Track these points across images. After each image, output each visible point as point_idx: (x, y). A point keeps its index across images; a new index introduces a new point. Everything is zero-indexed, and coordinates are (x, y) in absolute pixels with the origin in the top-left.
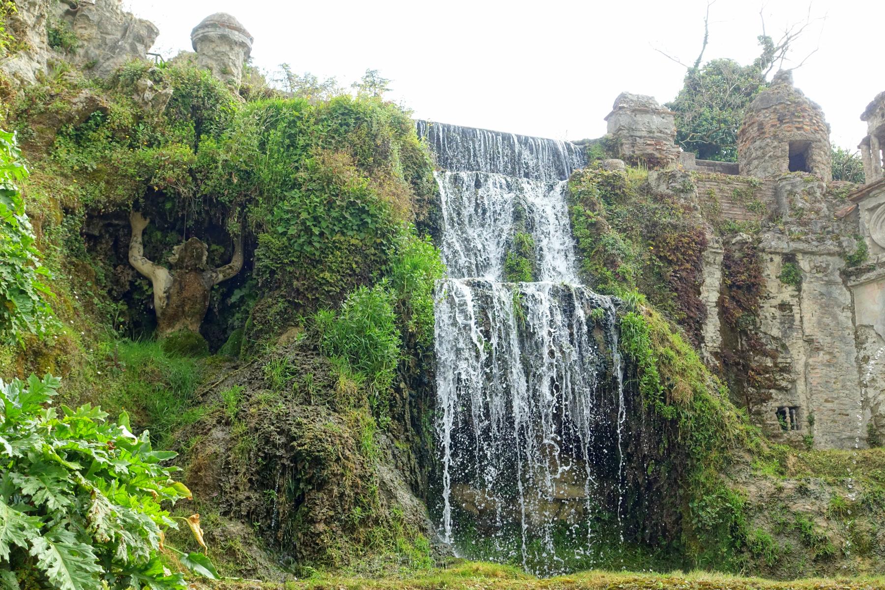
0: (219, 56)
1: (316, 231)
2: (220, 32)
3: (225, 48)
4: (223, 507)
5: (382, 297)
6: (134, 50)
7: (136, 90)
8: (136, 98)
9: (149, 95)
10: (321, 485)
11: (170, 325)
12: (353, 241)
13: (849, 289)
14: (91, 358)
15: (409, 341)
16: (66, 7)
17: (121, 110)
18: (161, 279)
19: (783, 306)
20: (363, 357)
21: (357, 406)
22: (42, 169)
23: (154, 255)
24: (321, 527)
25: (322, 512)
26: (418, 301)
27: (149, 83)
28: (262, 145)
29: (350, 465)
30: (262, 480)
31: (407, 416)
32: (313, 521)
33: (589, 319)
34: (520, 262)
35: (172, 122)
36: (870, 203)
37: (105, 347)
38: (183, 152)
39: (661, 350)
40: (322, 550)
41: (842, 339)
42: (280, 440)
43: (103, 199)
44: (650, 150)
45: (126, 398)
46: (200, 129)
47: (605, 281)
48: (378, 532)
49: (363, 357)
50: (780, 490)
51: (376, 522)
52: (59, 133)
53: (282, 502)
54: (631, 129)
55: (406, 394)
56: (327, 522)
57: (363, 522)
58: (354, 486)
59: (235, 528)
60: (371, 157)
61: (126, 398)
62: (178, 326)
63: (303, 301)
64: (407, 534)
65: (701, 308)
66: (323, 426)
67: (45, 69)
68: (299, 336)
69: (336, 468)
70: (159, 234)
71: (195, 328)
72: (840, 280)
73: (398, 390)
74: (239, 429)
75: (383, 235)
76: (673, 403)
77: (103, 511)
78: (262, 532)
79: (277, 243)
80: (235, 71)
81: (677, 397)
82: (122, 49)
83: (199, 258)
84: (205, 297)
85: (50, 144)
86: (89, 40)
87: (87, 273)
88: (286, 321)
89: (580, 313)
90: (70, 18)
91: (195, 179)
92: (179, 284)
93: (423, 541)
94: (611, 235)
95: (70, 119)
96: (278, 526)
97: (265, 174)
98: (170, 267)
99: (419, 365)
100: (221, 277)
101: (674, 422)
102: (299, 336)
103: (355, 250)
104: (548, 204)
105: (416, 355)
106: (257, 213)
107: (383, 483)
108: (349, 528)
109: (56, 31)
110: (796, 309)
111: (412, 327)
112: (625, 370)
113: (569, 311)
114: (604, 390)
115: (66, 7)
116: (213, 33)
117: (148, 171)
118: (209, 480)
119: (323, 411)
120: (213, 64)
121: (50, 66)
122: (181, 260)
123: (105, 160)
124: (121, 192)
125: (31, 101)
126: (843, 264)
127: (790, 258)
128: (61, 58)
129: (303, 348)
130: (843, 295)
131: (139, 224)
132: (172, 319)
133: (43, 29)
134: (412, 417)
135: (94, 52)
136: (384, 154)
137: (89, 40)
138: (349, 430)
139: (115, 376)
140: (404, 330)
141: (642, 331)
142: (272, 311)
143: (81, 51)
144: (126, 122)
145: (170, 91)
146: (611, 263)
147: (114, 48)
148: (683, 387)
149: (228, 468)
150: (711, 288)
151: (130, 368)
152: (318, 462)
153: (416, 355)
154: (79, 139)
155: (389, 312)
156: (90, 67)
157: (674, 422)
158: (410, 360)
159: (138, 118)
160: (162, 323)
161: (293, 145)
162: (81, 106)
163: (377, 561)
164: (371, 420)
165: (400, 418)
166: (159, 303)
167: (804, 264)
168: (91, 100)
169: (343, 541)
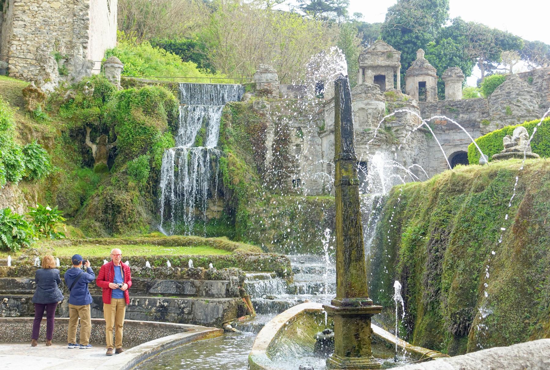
0: (112, 72)
1: (130, 136)
2: (111, 65)
3: (113, 70)
4: (96, 219)
5: (145, 158)
6: (86, 72)
7: (84, 90)
8: (83, 92)
9: (87, 91)
10: (119, 213)
11: (98, 162)
12: (143, 138)
13: (321, 138)
14: (69, 176)
15: (153, 170)
16: (65, 60)
17: (78, 98)
18: (94, 148)
19: (297, 145)
20: (137, 176)
21: (134, 190)
22: (55, 119)
23: (93, 141)
24: (118, 224)
25: (118, 220)
26: (156, 156)
27: (87, 87)
28: (119, 107)
29: (128, 207)
30: (105, 212)
31: (151, 191)
32: (117, 222)
33: (210, 159)
34: (202, 138)
35: (95, 99)
36: (326, 109)
37: (74, 172)
38: (96, 110)
39: (232, 168)
40: (118, 230)
41: (317, 156)
42: (109, 201)
43: (74, 126)
44: (266, 87)
45: (79, 187)
46: (104, 100)
47: (223, 144)
48: (134, 225)
49: (137, 176)
50: (258, 210)
51: (134, 222)
52: (61, 107)
53: (110, 217)
54: (259, 80)
55: (151, 185)
56: (121, 222)
57: (131, 222)
58: (129, 212)
59: (97, 224)
60: (150, 109)
61: (79, 187)
62: (100, 162)
63: (129, 157)
64: (143, 225)
65: (265, 148)
66: (122, 197)
67: (57, 84)
68: (123, 169)
69: (123, 208)
70: (94, 133)
71: (105, 162)
72: (317, 135)
73: (149, 184)
74: (101, 198)
75: (152, 135)
76: (233, 184)
77: (15, 231)
78: (105, 225)
79: (121, 139)
80: (117, 76)
81: (234, 182)
82: (82, 73)
83: (105, 141)
84: (107, 153)
85: (58, 111)
86: (72, 70)
87: (71, 148)
88: (124, 162)
89: (208, 156)
90: (66, 63)
91: (100, 118)
92: (99, 149)
93: (148, 226)
94: (230, 128)
95: (63, 103)
96: (109, 223)
97: (118, 117)
98: (97, 144)
99: (157, 176)
100: (112, 146)
101: (233, 190)
102: (123, 169)
103: (144, 140)
104: (215, 116)
105: (156, 173)
106: (116, 128)
107: (138, 212)
108: (126, 223)
109: (61, 69)
110: (302, 146)
111: (154, 166)
112: (219, 175)
113: (205, 156)
114: (212, 179)
115: (65, 60)
116: (109, 65)
117: (86, 117)
118: (93, 212)
119: (124, 192)
120: (110, 75)
121: (59, 83)
122: (99, 142)
123: (75, 113)
124: (79, 124)
125: (52, 97)
126: (318, 130)
127: (299, 129)
128: (63, 79)
129: (123, 173)
130: (318, 140)
131: (89, 130)
132: (99, 160)
133: (56, 71)
134: (153, 192)
135: (74, 74)
136: (156, 106)
137: (72, 70)
138: (130, 198)
139: (76, 180)
140: (151, 166)
141: (225, 162)
142: (120, 159)
143: (69, 75)
144: (80, 101)
145: (93, 90)
146: (227, 138)
147: (79, 73)
148: (237, 179)
149: (97, 209)
150: (270, 140)
151: (80, 178)
152: (119, 207)
153: (156, 173)
154: (67, 107)
155: (146, 162)
156: (73, 79)
157: (233, 190)
158: (154, 175)
159: (84, 99)
160: (96, 161)
161: (128, 106)
162: (66, 98)
163: (133, 232)
164: (138, 194)
165: (149, 192)
166: (94, 155)
167: (304, 131)
168: (69, 95)
169: (125, 227)
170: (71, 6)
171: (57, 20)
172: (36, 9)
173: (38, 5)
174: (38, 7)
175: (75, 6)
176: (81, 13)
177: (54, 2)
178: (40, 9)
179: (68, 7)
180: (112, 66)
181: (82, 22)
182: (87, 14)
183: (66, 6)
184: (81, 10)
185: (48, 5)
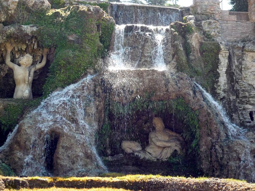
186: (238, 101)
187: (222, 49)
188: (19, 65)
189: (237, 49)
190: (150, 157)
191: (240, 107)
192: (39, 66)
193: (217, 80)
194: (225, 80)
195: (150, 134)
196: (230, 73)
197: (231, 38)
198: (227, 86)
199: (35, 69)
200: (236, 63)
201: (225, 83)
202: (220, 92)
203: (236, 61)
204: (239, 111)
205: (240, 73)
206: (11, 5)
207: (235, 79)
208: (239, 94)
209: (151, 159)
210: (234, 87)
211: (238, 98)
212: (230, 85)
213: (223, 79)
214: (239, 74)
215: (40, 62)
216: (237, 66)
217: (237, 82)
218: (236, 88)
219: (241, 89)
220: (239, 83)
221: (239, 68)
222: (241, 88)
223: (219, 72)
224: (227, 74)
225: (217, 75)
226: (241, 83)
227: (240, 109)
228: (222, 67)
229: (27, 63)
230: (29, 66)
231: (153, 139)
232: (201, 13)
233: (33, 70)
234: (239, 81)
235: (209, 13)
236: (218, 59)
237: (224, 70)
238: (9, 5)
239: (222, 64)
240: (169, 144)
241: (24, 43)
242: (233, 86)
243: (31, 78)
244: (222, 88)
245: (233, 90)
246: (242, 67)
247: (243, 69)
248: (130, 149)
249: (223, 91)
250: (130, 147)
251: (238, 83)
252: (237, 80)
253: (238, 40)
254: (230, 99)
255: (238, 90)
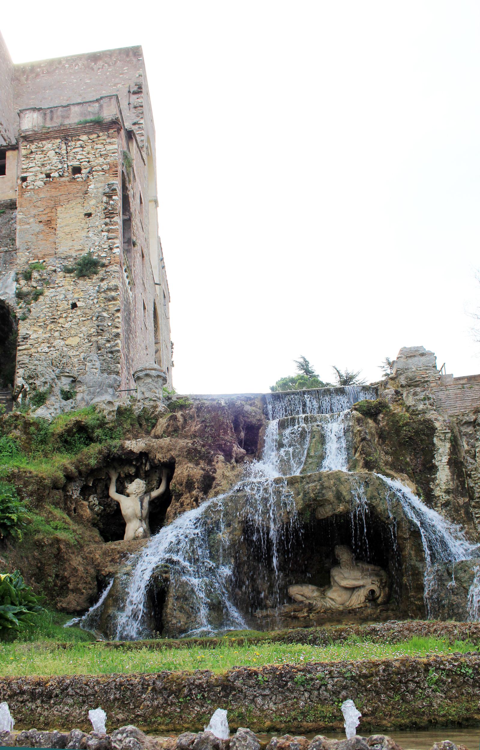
2: (144, 373)
116: (141, 374)
170: (94, 339)
171: (76, 360)
172: (47, 350)
173: (48, 345)
174: (48, 347)
175: (100, 337)
176: (108, 345)
177: (71, 338)
178: (52, 349)
179: (90, 341)
180: (147, 375)
181: (110, 355)
182: (117, 344)
183: (86, 341)
184: (108, 341)
185: (62, 343)
186: (473, 504)
187: (438, 429)
188: (128, 496)
189: (465, 426)
190: (332, 605)
191: (476, 514)
192: (155, 493)
193: (433, 476)
194: (447, 476)
195: (332, 570)
196: (456, 464)
197: (455, 411)
198: (451, 483)
199: (150, 498)
200: (466, 447)
201: (447, 480)
202: (440, 494)
203: (465, 444)
204: (475, 519)
205: (474, 462)
206: (107, 417)
207: (466, 472)
208: (474, 493)
209: (333, 608)
210: (464, 485)
211: (473, 499)
212: (457, 481)
213: (443, 475)
214: (471, 463)
215: (157, 488)
216: (468, 452)
217: (470, 476)
218: (468, 484)
219: (477, 486)
220: (472, 476)
221: (470, 453)
222: (477, 483)
223: (437, 463)
224: (450, 466)
225: (433, 469)
226: (475, 476)
227: (477, 516)
228: (441, 456)
229: (137, 491)
230: (140, 495)
231: (336, 578)
232: (406, 385)
233: (146, 500)
234: (472, 473)
235: (419, 382)
236: (434, 445)
237: (445, 459)
238: (105, 417)
239: (440, 451)
240: (361, 583)
241: (131, 465)
242: (463, 483)
243: (145, 512)
244: (444, 487)
245: (463, 488)
246: (475, 451)
247: (477, 454)
248: (302, 595)
249: (445, 492)
250: (302, 593)
251: (470, 477)
252: (469, 473)
253: (467, 412)
254: (458, 503)
255: (472, 487)
